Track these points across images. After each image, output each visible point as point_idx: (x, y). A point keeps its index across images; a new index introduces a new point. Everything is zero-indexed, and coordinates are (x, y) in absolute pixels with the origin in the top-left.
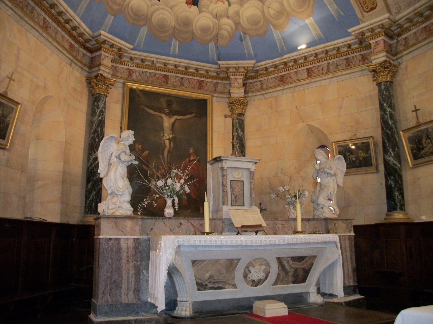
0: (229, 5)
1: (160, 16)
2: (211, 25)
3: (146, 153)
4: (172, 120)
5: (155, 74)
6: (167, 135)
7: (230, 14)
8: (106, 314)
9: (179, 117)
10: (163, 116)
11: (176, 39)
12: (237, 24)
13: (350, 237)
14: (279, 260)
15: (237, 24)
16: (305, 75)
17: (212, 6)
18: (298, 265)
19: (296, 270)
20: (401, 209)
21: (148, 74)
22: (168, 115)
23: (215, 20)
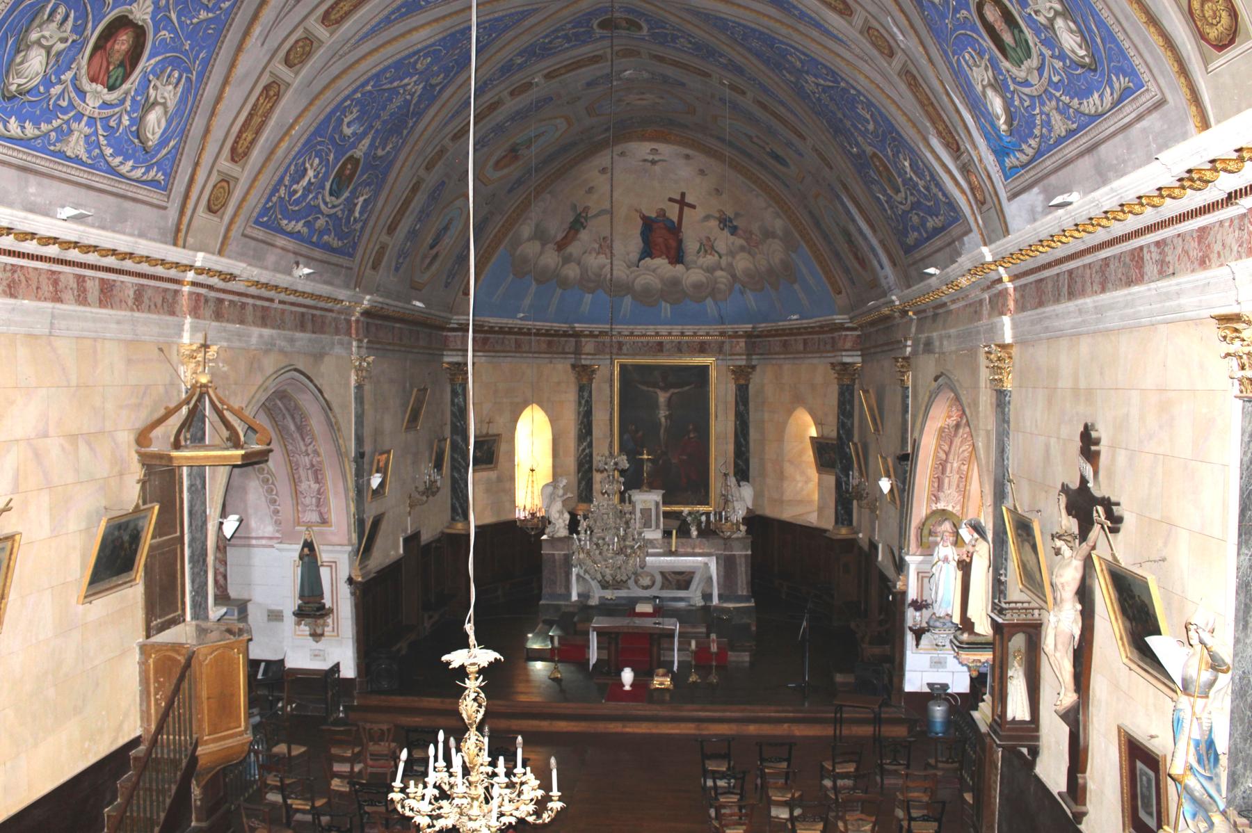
0: (720, 257)
1: (643, 282)
2: (704, 280)
3: (640, 433)
4: (668, 395)
5: (648, 343)
6: (662, 413)
7: (723, 266)
8: (547, 599)
9: (676, 391)
10: (658, 391)
11: (666, 301)
12: (734, 276)
13: (746, 555)
14: (662, 573)
15: (734, 276)
16: (801, 347)
17: (701, 261)
18: (680, 577)
19: (678, 581)
20: (843, 524)
21: (640, 344)
22: (664, 389)
23: (707, 274)
